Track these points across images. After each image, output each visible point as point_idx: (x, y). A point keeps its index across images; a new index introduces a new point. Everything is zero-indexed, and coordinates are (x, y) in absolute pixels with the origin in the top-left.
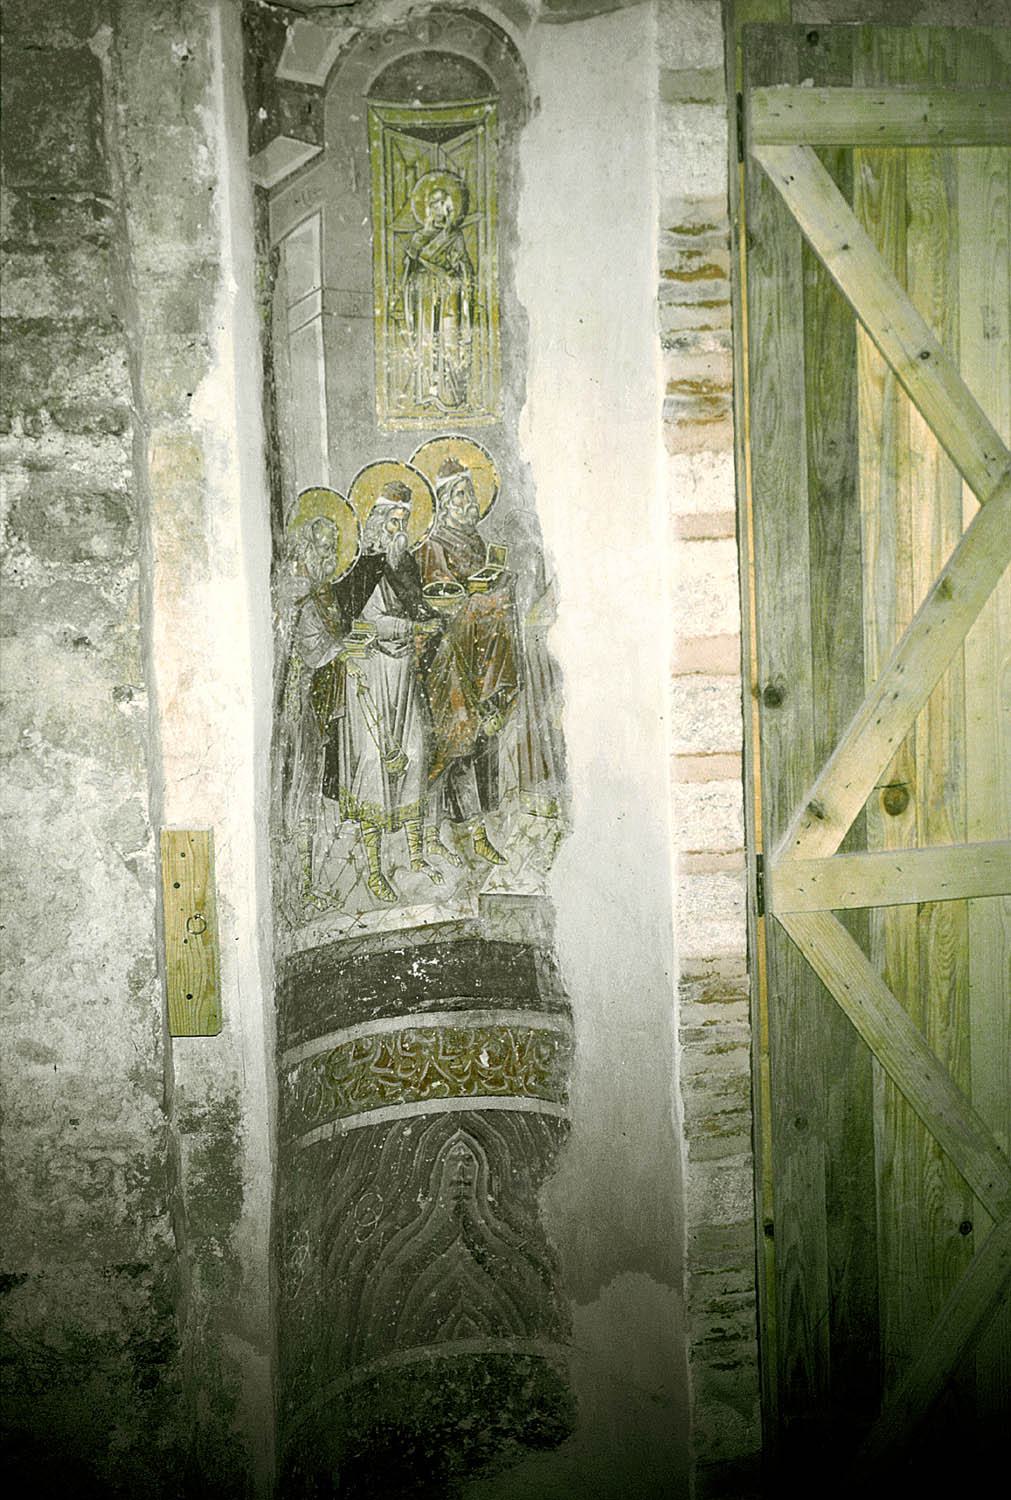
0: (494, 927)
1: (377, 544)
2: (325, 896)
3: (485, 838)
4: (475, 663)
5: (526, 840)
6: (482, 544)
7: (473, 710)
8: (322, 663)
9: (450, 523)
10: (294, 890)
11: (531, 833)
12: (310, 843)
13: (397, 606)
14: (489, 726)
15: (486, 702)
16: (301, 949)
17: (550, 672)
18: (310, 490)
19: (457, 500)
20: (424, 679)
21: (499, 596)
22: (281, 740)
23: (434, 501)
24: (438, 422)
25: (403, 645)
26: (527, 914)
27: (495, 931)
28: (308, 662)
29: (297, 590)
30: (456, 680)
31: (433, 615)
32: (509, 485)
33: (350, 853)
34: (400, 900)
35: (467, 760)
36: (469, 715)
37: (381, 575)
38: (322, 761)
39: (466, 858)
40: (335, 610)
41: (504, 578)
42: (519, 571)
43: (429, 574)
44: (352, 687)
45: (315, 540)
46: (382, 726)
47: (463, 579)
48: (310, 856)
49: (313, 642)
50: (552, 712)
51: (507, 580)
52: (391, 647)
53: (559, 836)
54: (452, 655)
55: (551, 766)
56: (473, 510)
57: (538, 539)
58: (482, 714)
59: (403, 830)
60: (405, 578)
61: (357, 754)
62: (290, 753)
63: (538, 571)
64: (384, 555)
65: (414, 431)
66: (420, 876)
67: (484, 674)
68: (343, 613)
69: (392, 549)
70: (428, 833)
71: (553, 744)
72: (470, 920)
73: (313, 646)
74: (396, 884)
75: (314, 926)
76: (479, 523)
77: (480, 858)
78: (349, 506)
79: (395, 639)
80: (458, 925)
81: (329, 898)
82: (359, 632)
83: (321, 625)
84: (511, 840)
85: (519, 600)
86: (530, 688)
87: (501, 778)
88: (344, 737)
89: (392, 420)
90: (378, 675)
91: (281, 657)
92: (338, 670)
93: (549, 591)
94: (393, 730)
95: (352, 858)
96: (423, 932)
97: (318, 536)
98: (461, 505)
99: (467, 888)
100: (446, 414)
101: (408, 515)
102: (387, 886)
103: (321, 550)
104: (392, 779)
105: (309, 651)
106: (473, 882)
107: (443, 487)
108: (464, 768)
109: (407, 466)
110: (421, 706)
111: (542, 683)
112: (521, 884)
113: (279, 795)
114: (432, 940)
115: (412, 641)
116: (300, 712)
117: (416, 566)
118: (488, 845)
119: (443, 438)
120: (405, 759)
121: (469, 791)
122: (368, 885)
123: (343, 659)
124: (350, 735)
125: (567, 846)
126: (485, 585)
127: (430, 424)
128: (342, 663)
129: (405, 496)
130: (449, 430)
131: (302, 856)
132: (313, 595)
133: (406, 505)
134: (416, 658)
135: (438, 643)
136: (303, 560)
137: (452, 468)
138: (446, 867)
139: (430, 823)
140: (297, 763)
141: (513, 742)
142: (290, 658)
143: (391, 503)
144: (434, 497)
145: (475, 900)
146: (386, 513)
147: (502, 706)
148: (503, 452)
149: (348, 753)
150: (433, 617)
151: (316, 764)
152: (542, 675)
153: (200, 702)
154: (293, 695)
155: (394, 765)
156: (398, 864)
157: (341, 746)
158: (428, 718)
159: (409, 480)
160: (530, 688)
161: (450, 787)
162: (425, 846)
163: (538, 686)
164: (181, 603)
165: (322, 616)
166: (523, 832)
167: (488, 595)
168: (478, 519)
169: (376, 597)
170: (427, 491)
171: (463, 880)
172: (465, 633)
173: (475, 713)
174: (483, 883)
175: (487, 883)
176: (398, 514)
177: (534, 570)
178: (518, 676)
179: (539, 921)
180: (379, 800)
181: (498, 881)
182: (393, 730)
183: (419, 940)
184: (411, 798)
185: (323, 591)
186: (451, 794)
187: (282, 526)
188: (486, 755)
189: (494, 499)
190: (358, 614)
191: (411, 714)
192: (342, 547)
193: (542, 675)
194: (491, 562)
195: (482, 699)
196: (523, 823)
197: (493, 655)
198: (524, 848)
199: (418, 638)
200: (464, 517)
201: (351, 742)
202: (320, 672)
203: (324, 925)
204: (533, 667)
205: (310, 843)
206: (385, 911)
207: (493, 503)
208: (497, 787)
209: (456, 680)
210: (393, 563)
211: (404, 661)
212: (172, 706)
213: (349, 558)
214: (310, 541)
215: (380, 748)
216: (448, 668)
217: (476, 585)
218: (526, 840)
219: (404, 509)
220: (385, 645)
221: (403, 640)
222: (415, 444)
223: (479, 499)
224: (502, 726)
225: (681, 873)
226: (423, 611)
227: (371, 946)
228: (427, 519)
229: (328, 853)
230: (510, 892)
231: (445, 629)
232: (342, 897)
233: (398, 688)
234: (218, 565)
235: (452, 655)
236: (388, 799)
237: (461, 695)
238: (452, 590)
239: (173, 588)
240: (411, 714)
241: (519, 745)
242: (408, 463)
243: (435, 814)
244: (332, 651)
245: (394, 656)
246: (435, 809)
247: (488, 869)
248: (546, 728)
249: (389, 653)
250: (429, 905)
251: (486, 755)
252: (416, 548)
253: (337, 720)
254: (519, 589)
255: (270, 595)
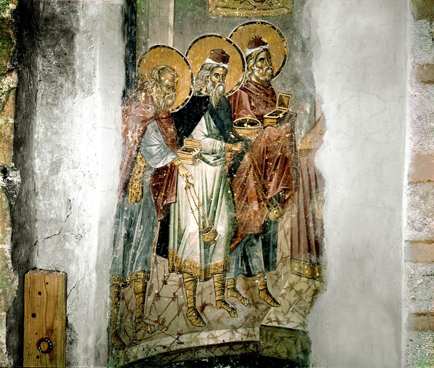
0: (268, 347)
1: (204, 89)
2: (153, 323)
3: (267, 289)
4: (265, 172)
5: (293, 292)
6: (274, 94)
7: (262, 203)
8: (160, 165)
9: (254, 79)
10: (129, 320)
11: (298, 288)
12: (145, 287)
13: (216, 131)
14: (273, 214)
15: (271, 198)
16: (132, 360)
17: (316, 181)
18: (158, 46)
19: (259, 64)
20: (231, 181)
21: (284, 127)
22: (125, 214)
23: (244, 64)
24: (250, 12)
25: (218, 158)
26: (291, 341)
27: (269, 350)
28: (150, 163)
29: (144, 113)
30: (252, 184)
31: (239, 139)
32: (294, 54)
33: (174, 294)
34: (208, 326)
35: (257, 236)
36: (259, 207)
37: (205, 110)
38: (157, 231)
39: (253, 301)
40: (172, 130)
41: (288, 116)
42: (298, 112)
43: (238, 112)
44: (182, 183)
45: (160, 81)
46: (201, 210)
47: (261, 118)
48: (144, 297)
49: (154, 150)
50: (316, 206)
51: (289, 117)
52: (211, 158)
53: (316, 292)
54: (251, 167)
55: (313, 242)
56: (269, 71)
57: (312, 90)
58: (268, 206)
59: (212, 280)
60: (222, 115)
61: (183, 228)
62: (131, 224)
63: (311, 111)
64: (208, 97)
65: (233, 17)
66: (223, 310)
67: (271, 180)
68: (179, 133)
69: (214, 93)
70: (229, 284)
71: (315, 229)
72: (254, 342)
73: (155, 152)
74: (205, 315)
75: (144, 344)
76: (273, 80)
77: (262, 301)
78: (186, 62)
79: (213, 153)
80: (245, 344)
81: (157, 325)
82: (189, 146)
83: (161, 139)
84: (283, 291)
85: (297, 132)
86: (301, 190)
87: (278, 250)
88: (174, 216)
89: (219, 9)
90: (200, 177)
91: (128, 156)
92: (172, 172)
93: (319, 125)
94: (208, 213)
95: (175, 297)
96: (222, 348)
97: (162, 78)
98: (261, 68)
99: (252, 321)
100: (255, 7)
101: (226, 72)
102: (198, 315)
103: (164, 89)
104: (207, 245)
105: (151, 156)
106: (257, 317)
107: (250, 55)
108: (255, 241)
109: (227, 40)
110: (228, 199)
111: (310, 187)
112: (288, 321)
113: (120, 253)
114: (227, 353)
115: (224, 156)
116: (142, 196)
117: (230, 106)
118: (268, 293)
119: (252, 23)
120: (216, 233)
121: (257, 257)
122: (187, 316)
123: (176, 164)
124: (179, 215)
125: (323, 299)
126: (275, 121)
127: (244, 13)
128: (175, 167)
129: (225, 59)
130: (256, 17)
131: (137, 296)
132: (156, 118)
133: (226, 66)
134: (226, 167)
135: (242, 158)
136: (150, 92)
137: (258, 42)
138: (238, 306)
139: (230, 276)
140: (138, 232)
141: (287, 226)
142: (135, 158)
143: (215, 64)
144: (245, 61)
145: (257, 329)
146: (211, 70)
147: (283, 202)
148: (291, 32)
149: (176, 227)
150: (239, 141)
151: (152, 232)
152: (310, 182)
153: (64, 184)
154: (136, 184)
155: (208, 237)
156: (208, 302)
157: (172, 222)
158: (233, 205)
159: (228, 50)
160: (301, 190)
161: (244, 252)
162: (226, 291)
163: (307, 188)
164: (56, 111)
165: (163, 133)
166: (291, 287)
167: (276, 128)
168: (272, 77)
169: (202, 125)
170: (240, 56)
171: (250, 315)
172: (260, 152)
173: (263, 206)
174: (263, 318)
175: (266, 318)
176: (220, 71)
177: (308, 110)
178: (294, 182)
179: (299, 347)
180: (197, 259)
181: (272, 317)
182: (208, 213)
183: (218, 353)
184: (218, 259)
185: (164, 116)
186: (245, 258)
187: (134, 66)
188: (269, 234)
189: (284, 64)
190: (188, 133)
191: (221, 204)
192: (180, 87)
193: (310, 182)
194: (279, 105)
195: (269, 196)
196: (291, 281)
197: (278, 167)
198: (291, 297)
199: (229, 154)
200: (263, 75)
201: (179, 219)
202: (159, 171)
203: (151, 343)
204: (304, 178)
205: (145, 287)
206: (197, 333)
207: (283, 66)
208: (276, 255)
209: (252, 184)
210: (214, 102)
211: (219, 168)
212: (44, 184)
213: (182, 97)
214: (157, 80)
215: (199, 224)
216: (247, 175)
217: (268, 121)
218: (293, 292)
219: (224, 68)
220: (206, 157)
221: (218, 154)
222: (234, 25)
223: (274, 63)
224: (281, 215)
225: (409, 329)
226: (233, 136)
227: (186, 355)
228: (238, 76)
229: (158, 296)
230: (280, 326)
231: (247, 149)
232: (166, 324)
233: (213, 186)
234: (81, 85)
235: (251, 167)
236: (203, 257)
237: (255, 194)
238: (252, 124)
239: (50, 101)
240: (221, 204)
241: (292, 228)
242: (228, 38)
243: (233, 271)
244: (169, 158)
245: (211, 165)
246: (234, 267)
247: (268, 309)
248: (311, 218)
249: (208, 163)
250: (224, 331)
251: (269, 234)
252: (230, 94)
253: (171, 203)
254: (297, 124)
255: (120, 111)
